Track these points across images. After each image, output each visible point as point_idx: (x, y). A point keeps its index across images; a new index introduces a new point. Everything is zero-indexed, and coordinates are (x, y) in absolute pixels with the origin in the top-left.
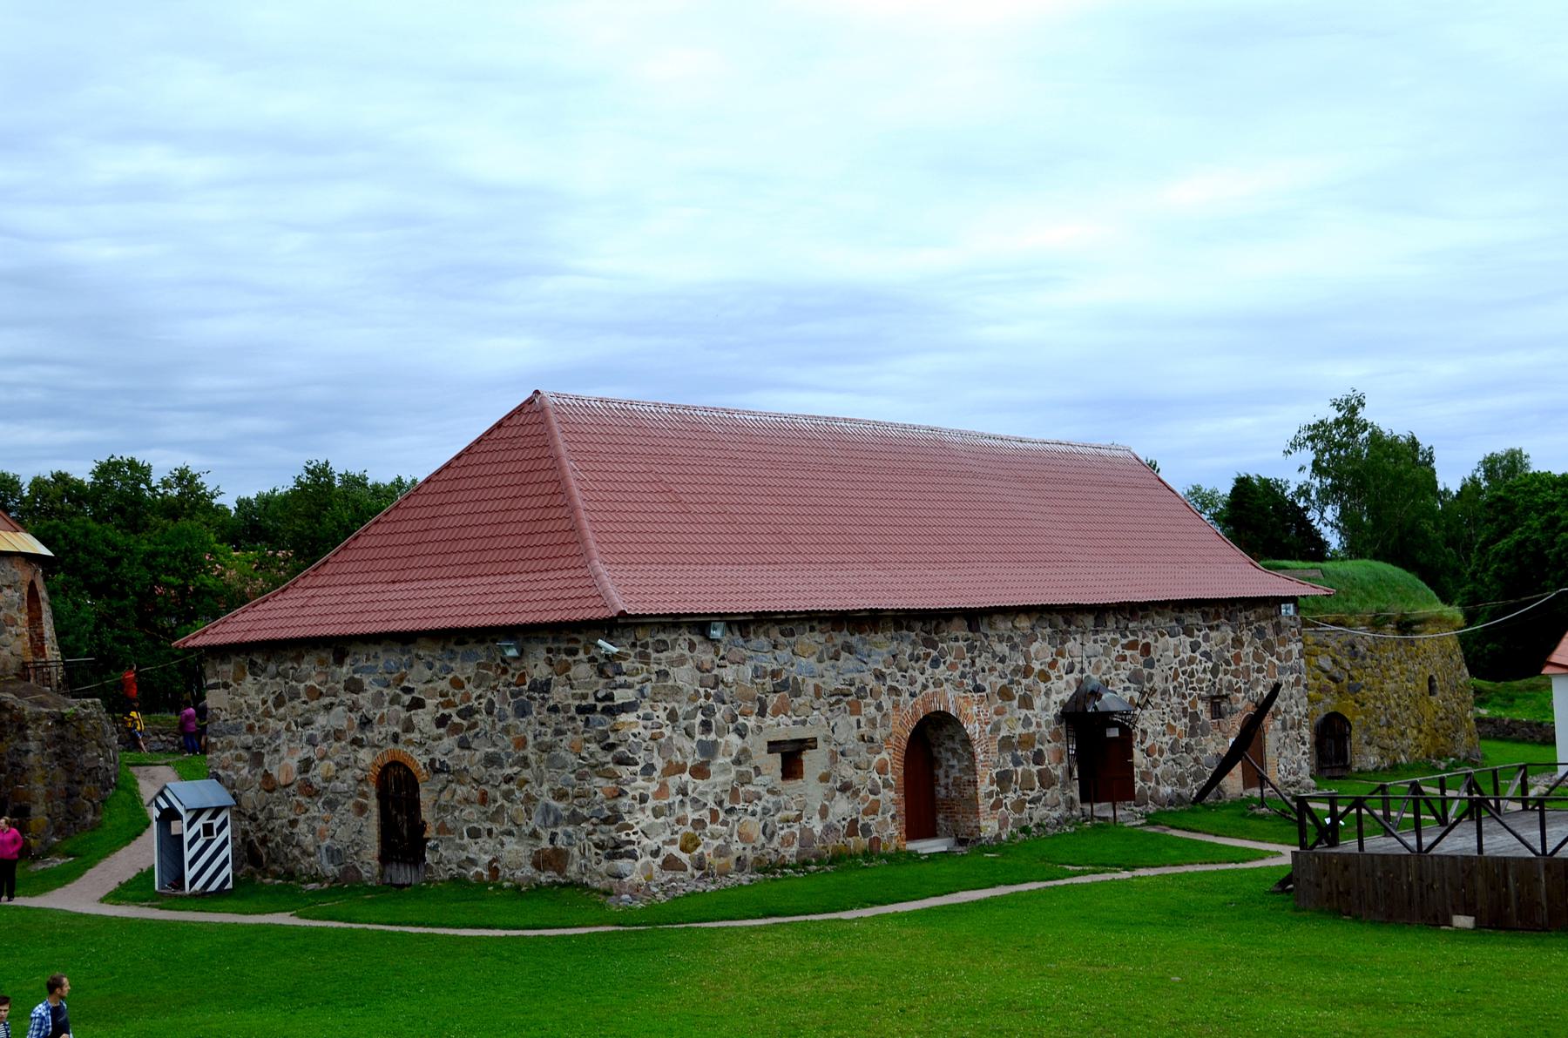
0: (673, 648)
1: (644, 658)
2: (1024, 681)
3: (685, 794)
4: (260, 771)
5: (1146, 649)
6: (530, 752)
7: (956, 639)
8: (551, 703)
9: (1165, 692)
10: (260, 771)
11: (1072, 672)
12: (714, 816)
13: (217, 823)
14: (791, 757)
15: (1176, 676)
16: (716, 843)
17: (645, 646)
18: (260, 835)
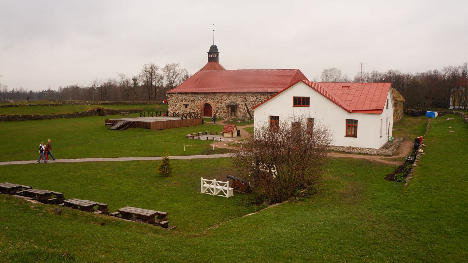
1: (170, 96)
2: (221, 101)
5: (245, 98)
14: (186, 106)
15: (252, 102)
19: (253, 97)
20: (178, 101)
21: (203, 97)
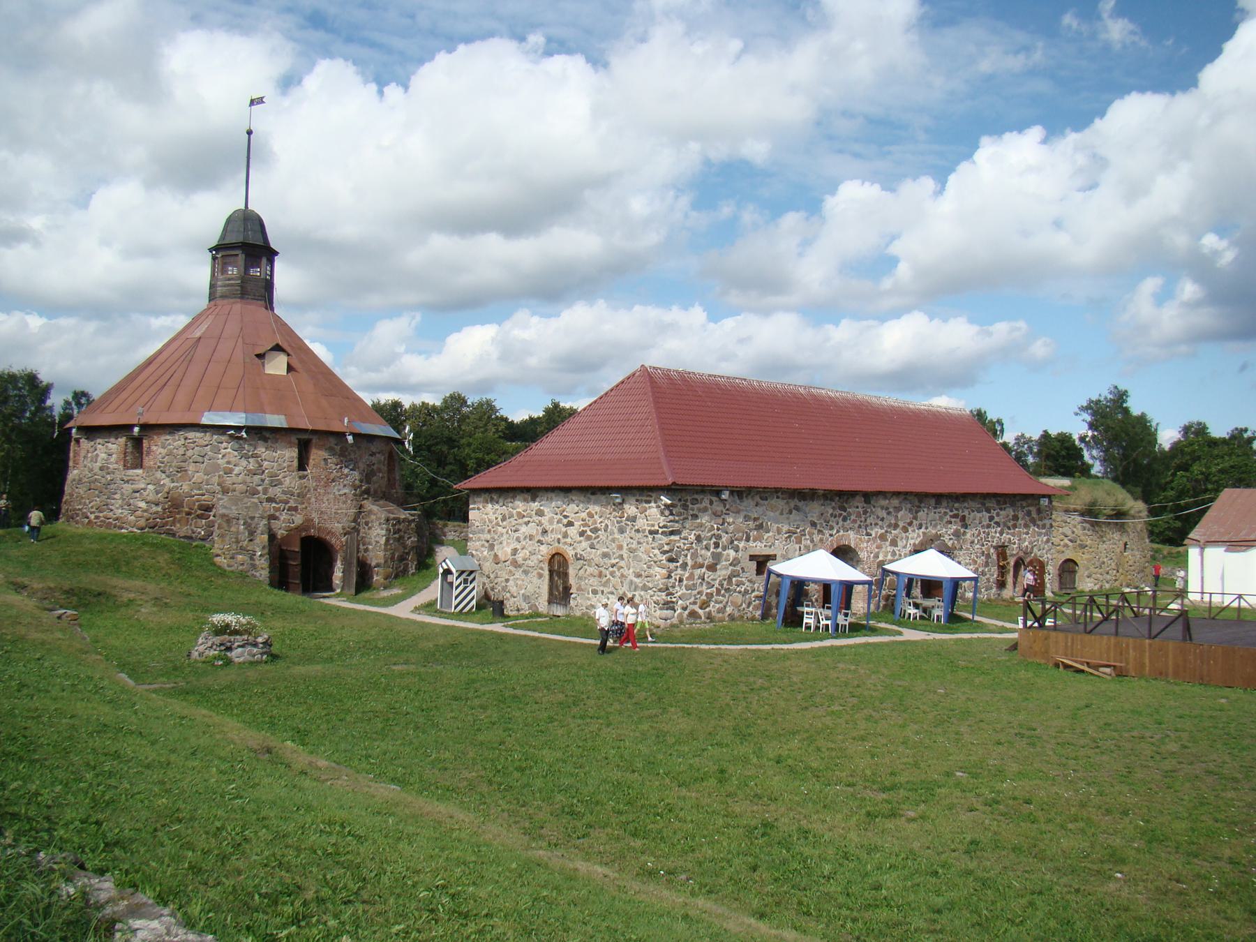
0: (701, 503)
3: (703, 579)
4: (493, 553)
6: (625, 553)
7: (857, 507)
8: (636, 527)
9: (972, 542)
10: (493, 553)
11: (921, 528)
12: (718, 591)
13: (470, 578)
16: (718, 606)
17: (686, 501)
18: (491, 585)
20: (725, 539)
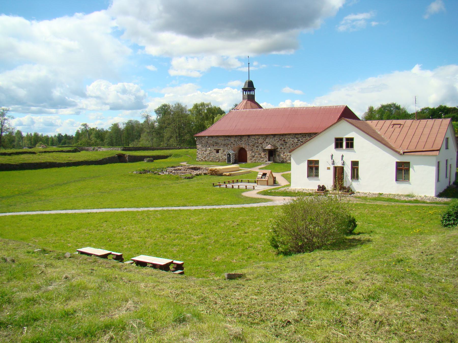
1: (200, 140)
5: (284, 141)
14: (218, 151)
19: (293, 139)
21: (237, 140)
